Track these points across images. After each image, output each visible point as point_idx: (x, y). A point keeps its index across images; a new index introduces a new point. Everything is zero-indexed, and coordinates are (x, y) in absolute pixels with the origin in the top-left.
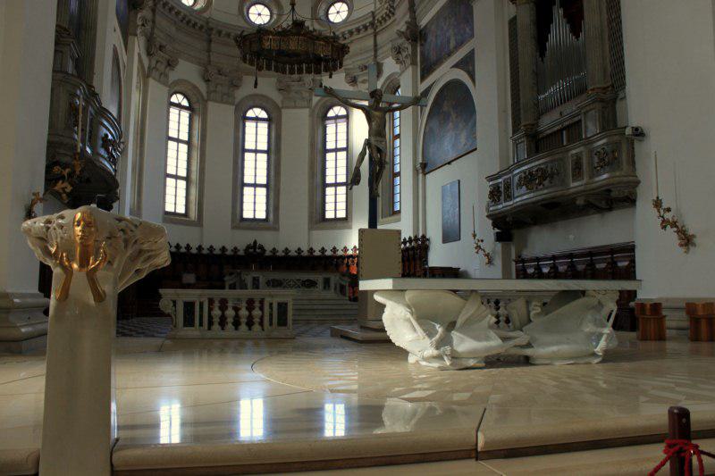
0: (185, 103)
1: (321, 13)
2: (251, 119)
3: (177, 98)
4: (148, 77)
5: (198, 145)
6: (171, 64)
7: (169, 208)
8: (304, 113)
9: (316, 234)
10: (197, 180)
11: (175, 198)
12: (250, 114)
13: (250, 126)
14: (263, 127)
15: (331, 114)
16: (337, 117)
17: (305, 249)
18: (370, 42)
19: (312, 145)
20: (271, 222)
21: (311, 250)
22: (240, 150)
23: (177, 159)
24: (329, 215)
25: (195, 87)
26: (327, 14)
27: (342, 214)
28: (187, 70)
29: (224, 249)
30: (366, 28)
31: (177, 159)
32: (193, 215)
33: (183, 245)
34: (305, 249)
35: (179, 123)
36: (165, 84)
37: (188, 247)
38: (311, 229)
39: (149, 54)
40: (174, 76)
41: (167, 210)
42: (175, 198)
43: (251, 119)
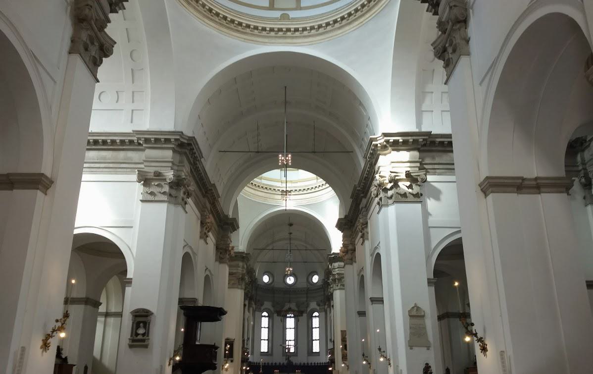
0: (267, 315)
1: (310, 280)
2: (289, 317)
3: (265, 314)
4: (255, 311)
5: (271, 328)
6: (262, 305)
7: (262, 350)
8: (306, 314)
9: (309, 357)
10: (270, 340)
11: (264, 347)
12: (288, 315)
13: (288, 319)
14: (293, 319)
15: (314, 315)
16: (316, 316)
17: (306, 363)
18: (323, 293)
19: (308, 326)
20: (295, 354)
21: (308, 364)
22: (284, 328)
23: (265, 334)
24: (314, 351)
25: (269, 309)
26: (312, 279)
27: (318, 351)
28: (267, 304)
29: (280, 363)
30: (321, 288)
31: (265, 334)
32: (270, 352)
33: (267, 363)
34: (306, 363)
35: (265, 322)
36: (260, 311)
37: (268, 363)
38: (308, 356)
39: (255, 304)
40: (262, 308)
41: (262, 351)
42: (264, 347)
43: (289, 317)
